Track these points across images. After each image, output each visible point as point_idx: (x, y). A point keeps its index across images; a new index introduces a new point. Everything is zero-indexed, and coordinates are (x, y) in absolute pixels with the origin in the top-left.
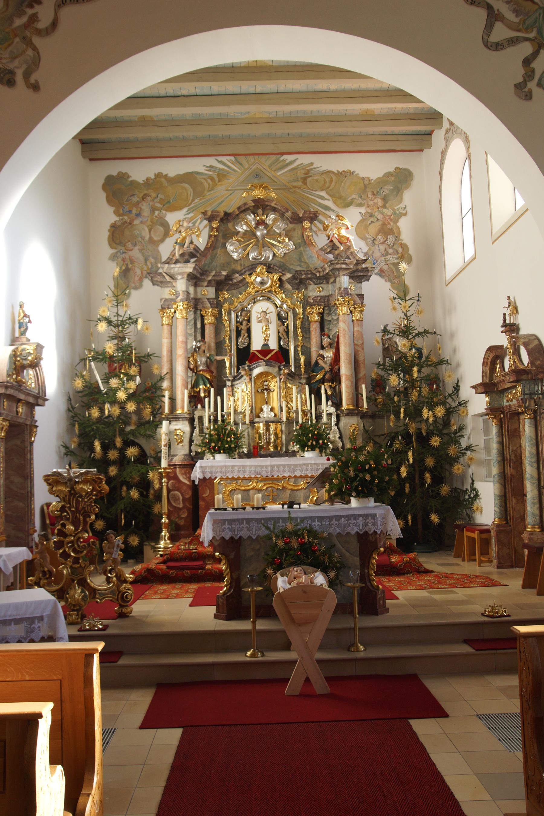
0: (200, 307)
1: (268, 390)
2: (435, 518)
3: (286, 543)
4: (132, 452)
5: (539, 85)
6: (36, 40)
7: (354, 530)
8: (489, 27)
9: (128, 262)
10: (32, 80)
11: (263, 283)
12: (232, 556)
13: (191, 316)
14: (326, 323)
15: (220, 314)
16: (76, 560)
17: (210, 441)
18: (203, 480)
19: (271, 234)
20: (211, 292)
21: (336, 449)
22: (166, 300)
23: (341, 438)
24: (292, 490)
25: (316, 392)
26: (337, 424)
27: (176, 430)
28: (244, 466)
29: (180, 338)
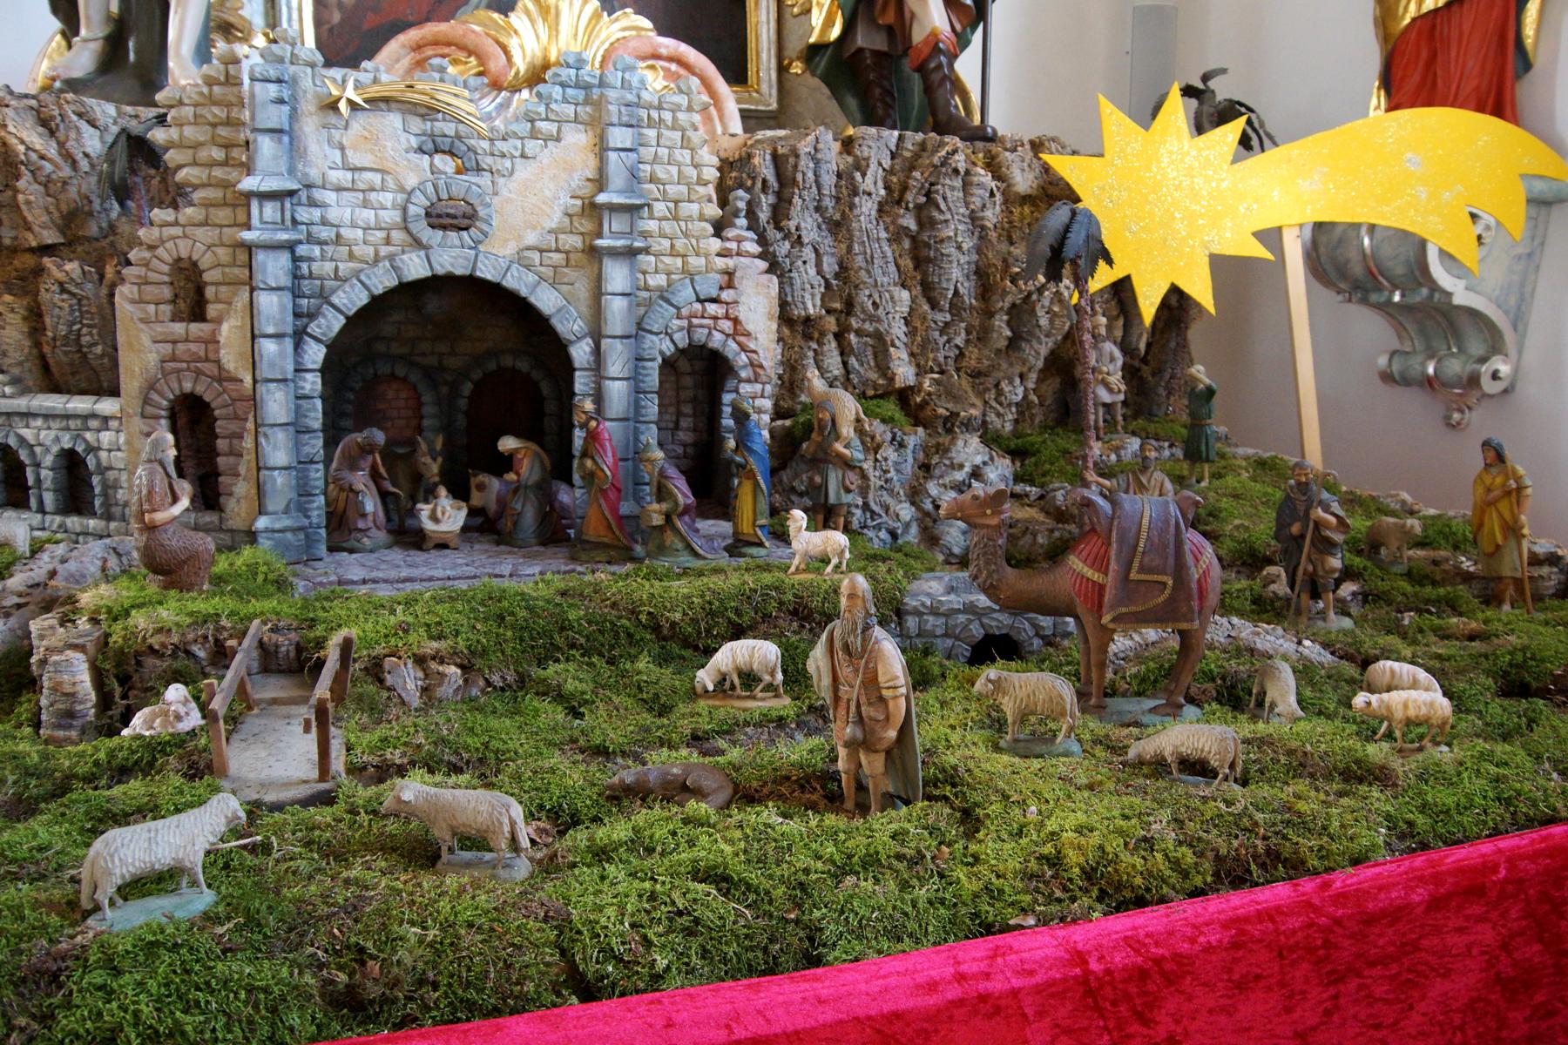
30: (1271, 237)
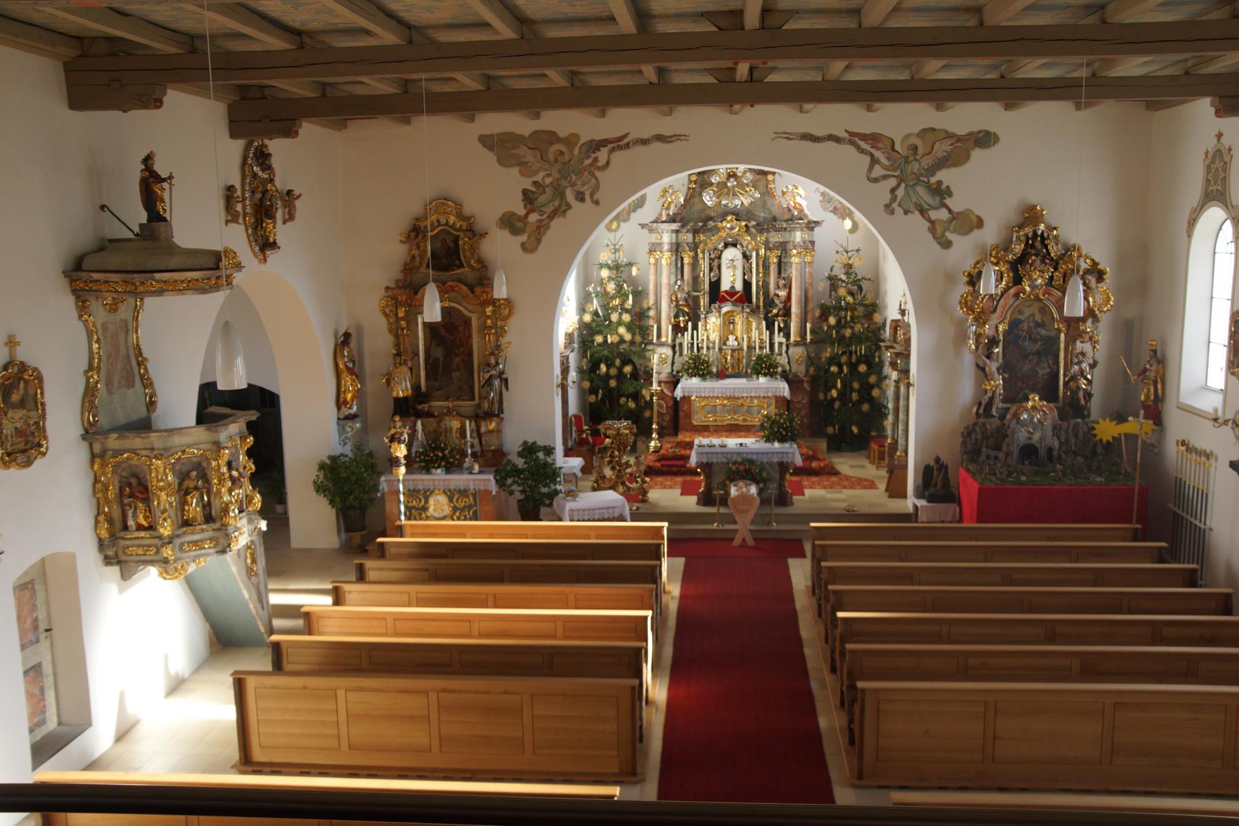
0: (680, 250)
1: (733, 323)
2: (855, 430)
3: (737, 468)
4: (628, 369)
5: (899, 205)
6: (597, 173)
7: (775, 460)
10: (595, 198)
11: (732, 228)
12: (707, 471)
13: (674, 258)
14: (783, 265)
15: (696, 254)
17: (688, 369)
18: (684, 398)
19: (741, 186)
20: (688, 238)
21: (784, 371)
22: (653, 244)
23: (789, 363)
24: (749, 406)
25: (770, 327)
26: (787, 352)
28: (713, 388)
29: (664, 281)
30: (1120, 435)
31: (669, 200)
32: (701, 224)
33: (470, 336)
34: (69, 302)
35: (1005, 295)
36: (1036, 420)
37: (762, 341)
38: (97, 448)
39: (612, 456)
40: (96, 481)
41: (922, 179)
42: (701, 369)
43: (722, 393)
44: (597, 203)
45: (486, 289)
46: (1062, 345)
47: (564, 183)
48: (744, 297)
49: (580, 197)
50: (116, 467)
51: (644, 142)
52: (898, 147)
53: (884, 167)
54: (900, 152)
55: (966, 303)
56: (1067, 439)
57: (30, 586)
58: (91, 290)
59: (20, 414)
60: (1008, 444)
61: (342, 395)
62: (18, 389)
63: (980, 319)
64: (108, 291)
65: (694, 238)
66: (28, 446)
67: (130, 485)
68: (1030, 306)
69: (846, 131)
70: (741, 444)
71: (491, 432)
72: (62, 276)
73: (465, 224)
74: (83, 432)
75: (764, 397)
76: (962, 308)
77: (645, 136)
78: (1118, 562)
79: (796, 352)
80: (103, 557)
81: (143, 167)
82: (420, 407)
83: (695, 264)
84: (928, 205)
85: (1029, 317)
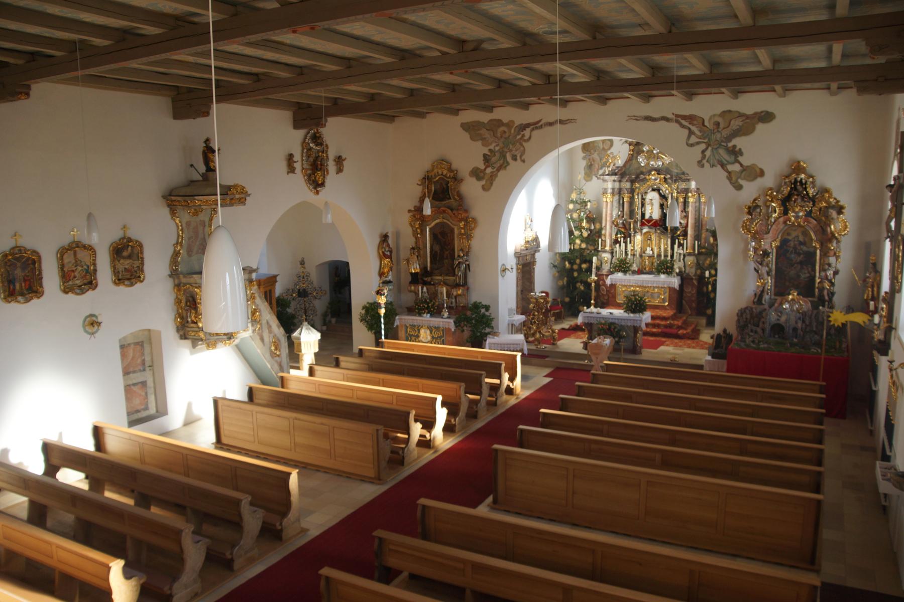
0: (622, 192)
1: (650, 240)
3: (602, 327)
6: (524, 144)
8: (689, 137)
9: (591, 160)
10: (523, 158)
11: (656, 179)
12: (589, 328)
14: (687, 203)
16: (538, 324)
21: (680, 272)
23: (685, 266)
26: (684, 259)
27: (604, 257)
28: (630, 280)
30: (846, 322)
31: (610, 161)
32: (633, 177)
33: (453, 239)
34: (166, 211)
35: (777, 222)
36: (795, 309)
37: (666, 250)
38: (177, 282)
39: (534, 315)
40: (177, 298)
41: (723, 144)
42: (623, 268)
43: (635, 283)
44: (524, 161)
45: (459, 212)
46: (818, 258)
47: (505, 150)
48: (660, 224)
49: (514, 158)
50: (185, 291)
51: (551, 124)
52: (706, 123)
53: (698, 137)
54: (708, 126)
55: (746, 226)
56: (811, 323)
57: (140, 344)
58: (174, 205)
59: (128, 261)
60: (763, 323)
61: (382, 270)
62: (127, 250)
63: (757, 237)
64: (180, 205)
65: (632, 185)
66: (133, 277)
67: (189, 301)
68: (795, 230)
69: (673, 114)
70: (611, 313)
71: (460, 295)
72: (162, 199)
73: (452, 174)
74: (170, 273)
75: (662, 287)
76: (743, 230)
77: (551, 120)
78: (803, 406)
79: (690, 260)
80: (179, 335)
81: (205, 145)
82: (426, 279)
83: (632, 202)
84: (726, 161)
85: (794, 238)
